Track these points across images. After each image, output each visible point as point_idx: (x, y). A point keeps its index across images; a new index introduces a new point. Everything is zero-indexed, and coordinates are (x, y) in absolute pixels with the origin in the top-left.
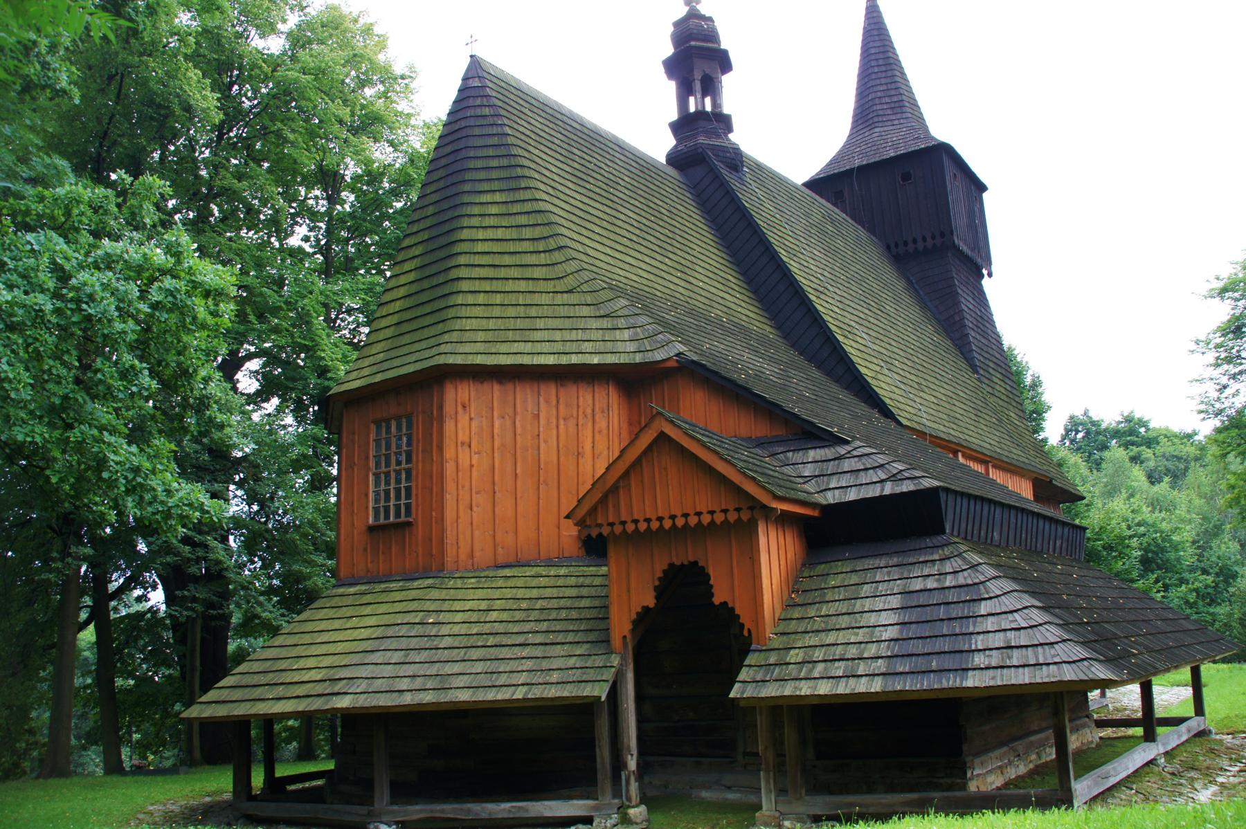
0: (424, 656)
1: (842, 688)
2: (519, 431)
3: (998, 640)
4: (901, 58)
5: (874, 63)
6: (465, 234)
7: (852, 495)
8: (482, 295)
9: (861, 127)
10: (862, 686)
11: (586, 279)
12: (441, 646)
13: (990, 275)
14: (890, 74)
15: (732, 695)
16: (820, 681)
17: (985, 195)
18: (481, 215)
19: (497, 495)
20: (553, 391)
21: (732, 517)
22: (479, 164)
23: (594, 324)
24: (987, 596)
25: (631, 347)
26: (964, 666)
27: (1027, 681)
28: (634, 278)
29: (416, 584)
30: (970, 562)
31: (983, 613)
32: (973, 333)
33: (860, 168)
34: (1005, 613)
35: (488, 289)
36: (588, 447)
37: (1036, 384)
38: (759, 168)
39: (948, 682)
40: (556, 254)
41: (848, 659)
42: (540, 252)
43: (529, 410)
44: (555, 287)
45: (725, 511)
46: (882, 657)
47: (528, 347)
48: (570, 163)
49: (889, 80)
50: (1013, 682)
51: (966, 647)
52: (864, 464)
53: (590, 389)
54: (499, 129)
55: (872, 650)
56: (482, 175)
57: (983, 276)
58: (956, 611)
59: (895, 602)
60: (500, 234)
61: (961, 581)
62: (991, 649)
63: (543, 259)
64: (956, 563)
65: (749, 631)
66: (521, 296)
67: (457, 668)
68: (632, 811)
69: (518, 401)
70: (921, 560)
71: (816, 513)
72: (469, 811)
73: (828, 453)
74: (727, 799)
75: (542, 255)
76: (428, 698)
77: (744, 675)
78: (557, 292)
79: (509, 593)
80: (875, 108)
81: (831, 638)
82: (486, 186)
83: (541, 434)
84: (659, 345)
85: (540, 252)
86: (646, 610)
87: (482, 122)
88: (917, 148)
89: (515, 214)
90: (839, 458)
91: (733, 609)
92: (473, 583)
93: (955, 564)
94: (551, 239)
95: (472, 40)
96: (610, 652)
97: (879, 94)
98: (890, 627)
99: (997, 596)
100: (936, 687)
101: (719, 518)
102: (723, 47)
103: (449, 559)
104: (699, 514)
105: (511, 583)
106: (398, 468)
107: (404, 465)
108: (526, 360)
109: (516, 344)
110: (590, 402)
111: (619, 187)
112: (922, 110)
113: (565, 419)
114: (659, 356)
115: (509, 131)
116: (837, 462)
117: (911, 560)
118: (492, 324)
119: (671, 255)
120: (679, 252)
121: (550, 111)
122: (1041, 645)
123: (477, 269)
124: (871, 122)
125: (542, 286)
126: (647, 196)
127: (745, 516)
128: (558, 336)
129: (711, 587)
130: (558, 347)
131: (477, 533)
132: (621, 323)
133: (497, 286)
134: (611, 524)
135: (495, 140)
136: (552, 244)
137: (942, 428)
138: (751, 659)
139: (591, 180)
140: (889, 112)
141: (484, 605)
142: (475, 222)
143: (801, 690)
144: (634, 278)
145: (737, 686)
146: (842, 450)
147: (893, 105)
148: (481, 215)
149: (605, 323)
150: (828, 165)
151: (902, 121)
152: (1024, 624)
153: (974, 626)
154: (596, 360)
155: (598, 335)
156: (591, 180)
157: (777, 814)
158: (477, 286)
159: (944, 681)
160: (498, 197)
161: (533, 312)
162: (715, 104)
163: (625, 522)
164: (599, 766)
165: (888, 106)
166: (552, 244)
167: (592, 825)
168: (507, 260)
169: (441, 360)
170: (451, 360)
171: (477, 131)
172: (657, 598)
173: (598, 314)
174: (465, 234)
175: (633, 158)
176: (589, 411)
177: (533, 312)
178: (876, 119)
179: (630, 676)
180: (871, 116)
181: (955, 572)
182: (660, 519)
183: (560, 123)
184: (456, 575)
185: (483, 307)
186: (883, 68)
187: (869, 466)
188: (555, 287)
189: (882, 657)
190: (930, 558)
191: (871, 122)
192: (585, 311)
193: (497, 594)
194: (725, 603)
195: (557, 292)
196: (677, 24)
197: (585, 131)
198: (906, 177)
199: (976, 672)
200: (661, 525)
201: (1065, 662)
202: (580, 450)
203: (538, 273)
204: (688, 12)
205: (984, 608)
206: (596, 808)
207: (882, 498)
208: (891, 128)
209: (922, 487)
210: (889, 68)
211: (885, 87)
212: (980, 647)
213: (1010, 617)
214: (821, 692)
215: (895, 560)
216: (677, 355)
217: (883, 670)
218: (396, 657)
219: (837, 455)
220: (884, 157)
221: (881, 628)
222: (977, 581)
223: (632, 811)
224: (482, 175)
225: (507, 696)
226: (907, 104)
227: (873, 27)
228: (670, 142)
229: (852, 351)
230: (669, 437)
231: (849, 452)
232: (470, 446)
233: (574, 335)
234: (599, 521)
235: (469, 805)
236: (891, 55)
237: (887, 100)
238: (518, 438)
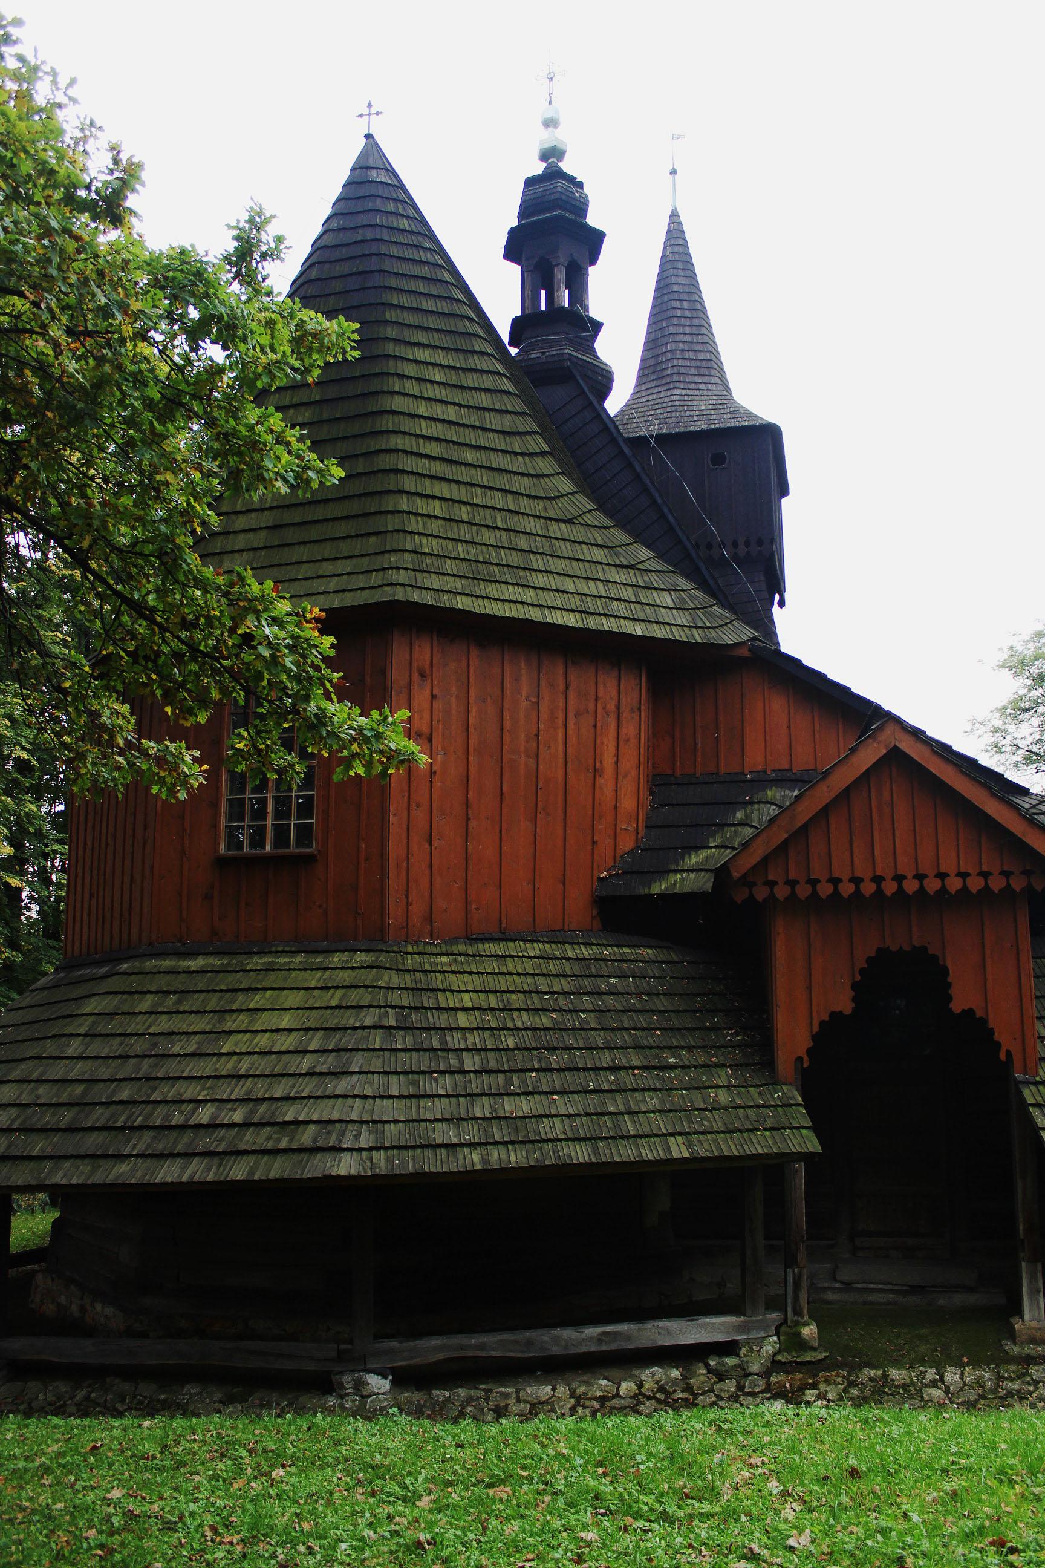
2: (507, 725)
5: (677, 304)
6: (399, 403)
13: (782, 604)
14: (696, 322)
18: (418, 379)
19: (473, 824)
20: (560, 670)
36: (608, 761)
42: (516, 454)
49: (695, 330)
53: (615, 674)
69: (507, 680)
72: (529, 1343)
80: (675, 362)
83: (541, 733)
85: (516, 454)
89: (470, 388)
91: (984, 1021)
95: (370, 111)
96: (775, 1082)
97: (681, 346)
101: (975, 884)
103: (394, 917)
108: (535, 615)
110: (614, 694)
129: (949, 985)
130: (575, 602)
131: (438, 881)
140: (693, 371)
147: (698, 363)
148: (418, 379)
151: (710, 387)
154: (638, 630)
155: (628, 593)
163: (861, 880)
165: (693, 364)
168: (470, 456)
170: (416, 597)
171: (394, 251)
172: (854, 1000)
176: (612, 706)
178: (676, 378)
180: (669, 372)
186: (688, 314)
194: (970, 1012)
196: (530, 182)
198: (718, 459)
200: (900, 888)
202: (598, 765)
206: (741, 1328)
208: (697, 393)
210: (695, 315)
211: (688, 338)
216: (752, 639)
220: (692, 428)
227: (676, 257)
234: (770, 877)
235: (528, 1334)
238: (506, 735)
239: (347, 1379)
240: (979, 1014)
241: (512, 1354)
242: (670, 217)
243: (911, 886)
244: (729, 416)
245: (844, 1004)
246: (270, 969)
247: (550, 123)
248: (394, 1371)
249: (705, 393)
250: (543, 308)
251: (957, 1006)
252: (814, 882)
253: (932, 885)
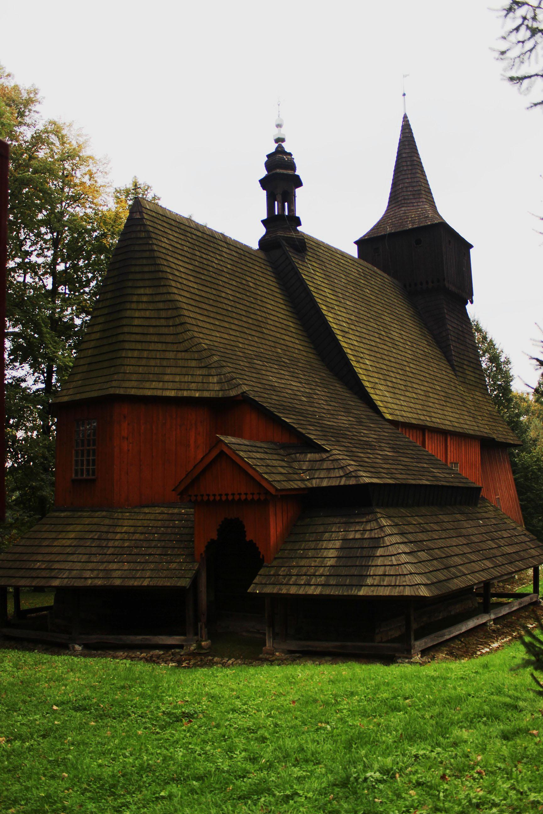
0: (99, 558)
1: (301, 592)
3: (380, 571)
4: (422, 161)
5: (404, 164)
6: (128, 313)
7: (325, 484)
8: (136, 351)
9: (394, 205)
10: (311, 591)
11: (195, 343)
12: (108, 553)
13: (472, 302)
15: (249, 591)
16: (292, 587)
17: (472, 250)
21: (256, 497)
22: (137, 269)
23: (199, 372)
24: (382, 545)
25: (217, 388)
26: (361, 584)
27: (387, 594)
28: (226, 336)
29: (97, 514)
30: (380, 525)
31: (378, 554)
32: (454, 344)
33: (391, 235)
34: (388, 556)
35: (140, 348)
37: (508, 362)
38: (319, 244)
39: (351, 591)
40: (179, 327)
41: (308, 575)
42: (170, 326)
44: (177, 348)
45: (253, 494)
46: (324, 575)
47: (160, 385)
48: (193, 262)
50: (381, 594)
51: (365, 573)
52: (334, 465)
54: (150, 247)
55: (321, 570)
56: (138, 276)
57: (467, 303)
58: (365, 553)
59: (338, 544)
60: (148, 314)
61: (373, 535)
62: (376, 575)
63: (172, 330)
64: (373, 525)
65: (263, 556)
66: (158, 353)
67: (115, 566)
68: (203, 643)
70: (356, 521)
73: (317, 456)
75: (171, 328)
76: (99, 582)
77: (256, 580)
78: (179, 351)
79: (146, 523)
80: (403, 194)
81: (303, 562)
82: (141, 284)
84: (233, 387)
85: (170, 326)
86: (212, 540)
87: (140, 242)
88: (426, 224)
90: (323, 460)
91: (255, 544)
93: (372, 525)
94: (176, 318)
97: (406, 185)
98: (332, 559)
99: (387, 546)
100: (345, 594)
101: (250, 497)
102: (296, 173)
104: (240, 494)
105: (148, 517)
106: (88, 448)
107: (92, 447)
109: (154, 383)
111: (223, 274)
112: (434, 196)
114: (233, 393)
115: (155, 248)
116: (320, 462)
117: (352, 520)
118: (141, 370)
119: (252, 316)
120: (259, 313)
121: (183, 227)
122: (400, 575)
123: (134, 335)
124: (400, 203)
125: (170, 347)
126: (241, 276)
127: (262, 498)
128: (177, 378)
129: (245, 532)
130: (177, 386)
132: (213, 371)
133: (145, 346)
134: (196, 496)
135: (147, 254)
136: (177, 321)
137: (415, 416)
138: (261, 572)
139: (206, 272)
140: (411, 197)
141: (132, 530)
142: (134, 306)
143: (282, 590)
144: (226, 336)
145: (252, 586)
146: (324, 456)
147: (414, 193)
149: (204, 372)
150: (372, 230)
151: (419, 204)
152: (395, 563)
153: (372, 562)
155: (200, 379)
156: (206, 272)
157: (273, 649)
158: (133, 346)
159: (350, 591)
160: (148, 291)
161: (165, 363)
162: (292, 209)
165: (411, 193)
166: (177, 321)
167: (183, 649)
168: (151, 330)
169: (112, 391)
170: (117, 392)
171: (137, 248)
173: (200, 366)
174: (128, 313)
175: (235, 249)
177: (165, 363)
178: (403, 202)
179: (204, 575)
180: (400, 199)
181: (371, 530)
182: (221, 495)
183: (189, 235)
184: (119, 511)
185: (137, 359)
186: (410, 168)
187: (336, 467)
188: (177, 348)
189: (324, 575)
190: (362, 520)
191: (400, 203)
192: (193, 364)
193: (139, 523)
195: (179, 351)
196: (268, 156)
197: (205, 236)
199: (366, 587)
200: (221, 498)
201: (408, 585)
203: (169, 339)
204: (277, 148)
205: (379, 552)
207: (339, 486)
208: (412, 208)
209: (359, 483)
212: (371, 574)
213: (390, 558)
214: (291, 592)
215: (344, 520)
217: (323, 582)
218: (85, 558)
219: (321, 459)
220: (405, 228)
221: (328, 559)
222: (380, 536)
223: (203, 643)
224: (138, 276)
225: (139, 584)
226: (423, 192)
228: (262, 231)
229: (360, 371)
230: (226, 454)
231: (328, 457)
233: (186, 379)
235: (121, 636)
236: (415, 158)
237: (411, 189)
239: (70, 645)
240: (254, 542)
242: (404, 118)
243: (230, 498)
244: (423, 219)
245: (214, 536)
246: (80, 517)
247: (279, 126)
249: (417, 207)
250: (276, 213)
251: (248, 539)
252: (202, 496)
253: (237, 497)
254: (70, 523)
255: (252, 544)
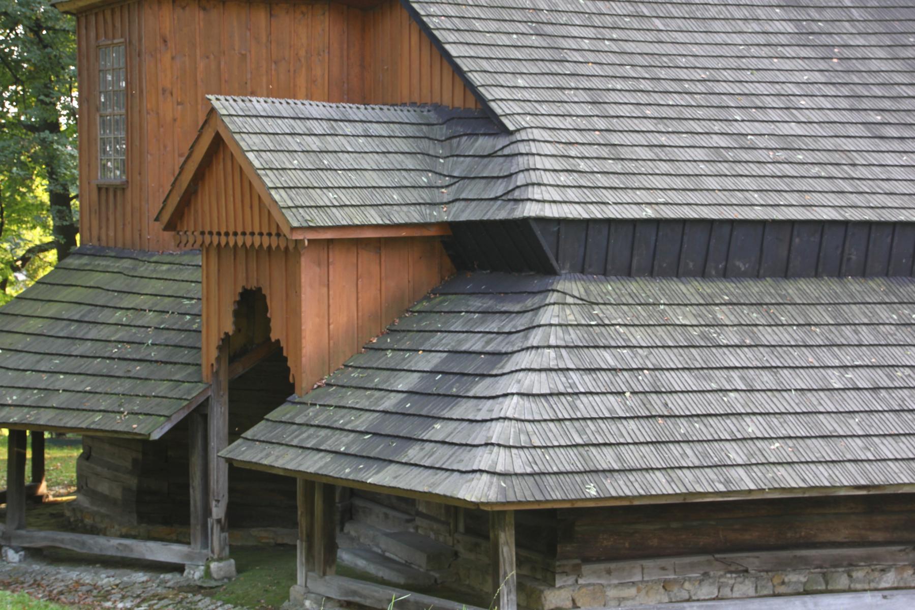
43: (236, 48)
71: (432, 232)
72: (83, 544)
74: (356, 565)
92: (162, 271)
113: (275, 63)
164: (192, 509)
206: (189, 556)
232: (172, 94)
241: (75, 549)
248: (24, 549)
254: (74, 283)
255: (277, 348)
